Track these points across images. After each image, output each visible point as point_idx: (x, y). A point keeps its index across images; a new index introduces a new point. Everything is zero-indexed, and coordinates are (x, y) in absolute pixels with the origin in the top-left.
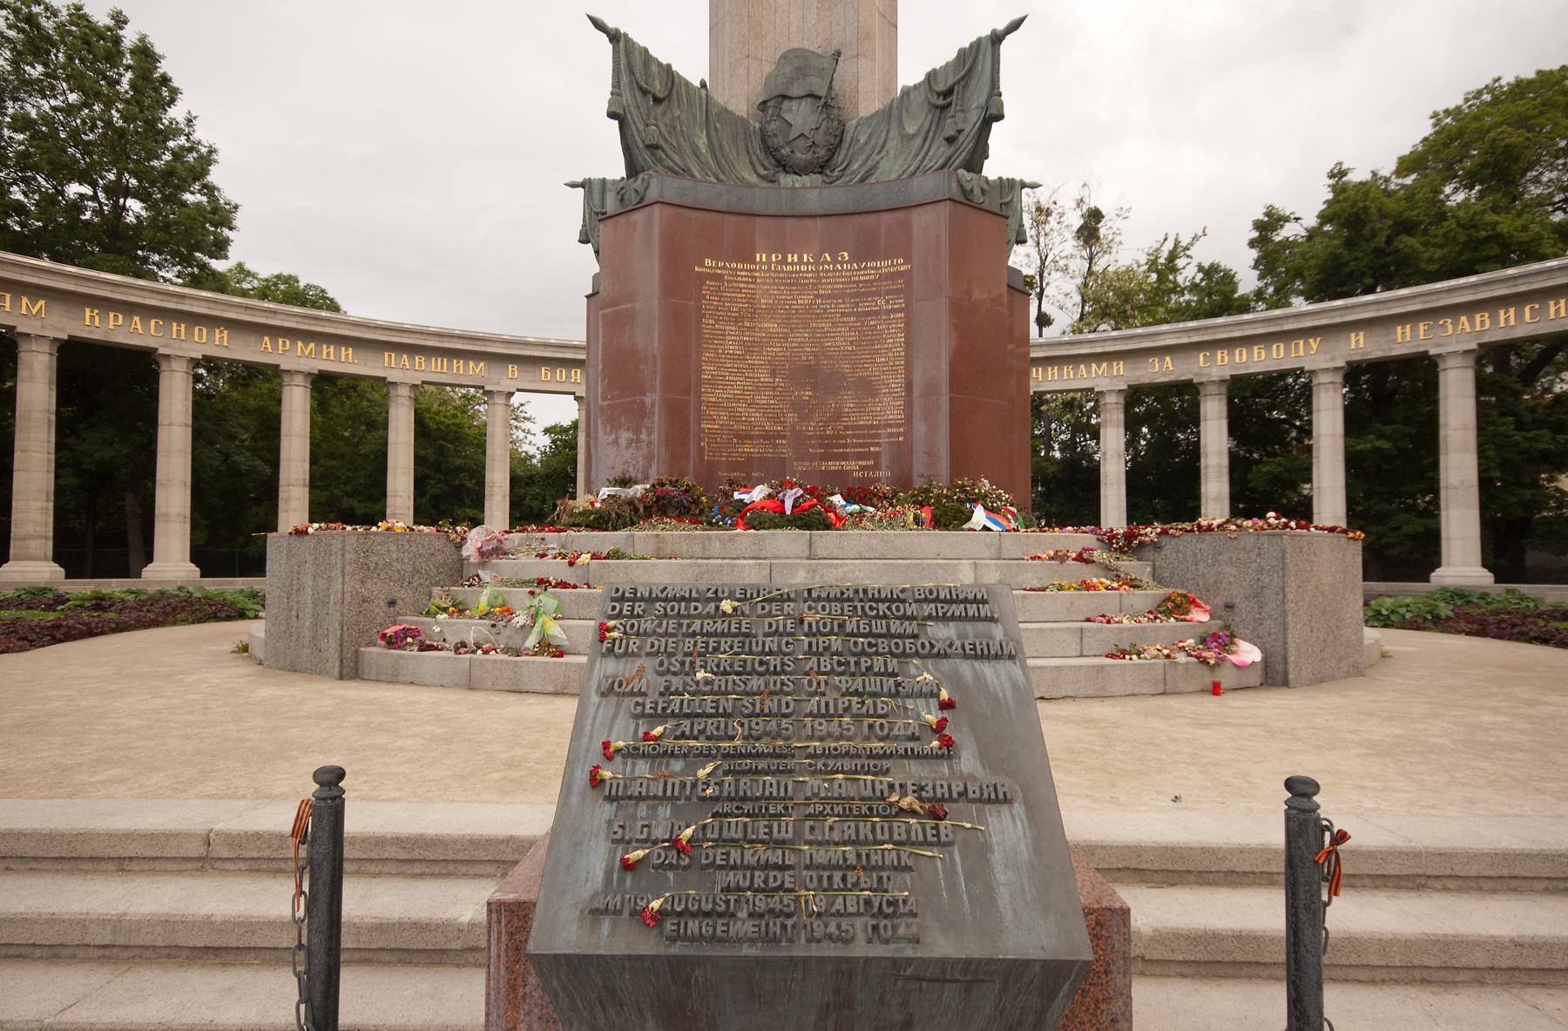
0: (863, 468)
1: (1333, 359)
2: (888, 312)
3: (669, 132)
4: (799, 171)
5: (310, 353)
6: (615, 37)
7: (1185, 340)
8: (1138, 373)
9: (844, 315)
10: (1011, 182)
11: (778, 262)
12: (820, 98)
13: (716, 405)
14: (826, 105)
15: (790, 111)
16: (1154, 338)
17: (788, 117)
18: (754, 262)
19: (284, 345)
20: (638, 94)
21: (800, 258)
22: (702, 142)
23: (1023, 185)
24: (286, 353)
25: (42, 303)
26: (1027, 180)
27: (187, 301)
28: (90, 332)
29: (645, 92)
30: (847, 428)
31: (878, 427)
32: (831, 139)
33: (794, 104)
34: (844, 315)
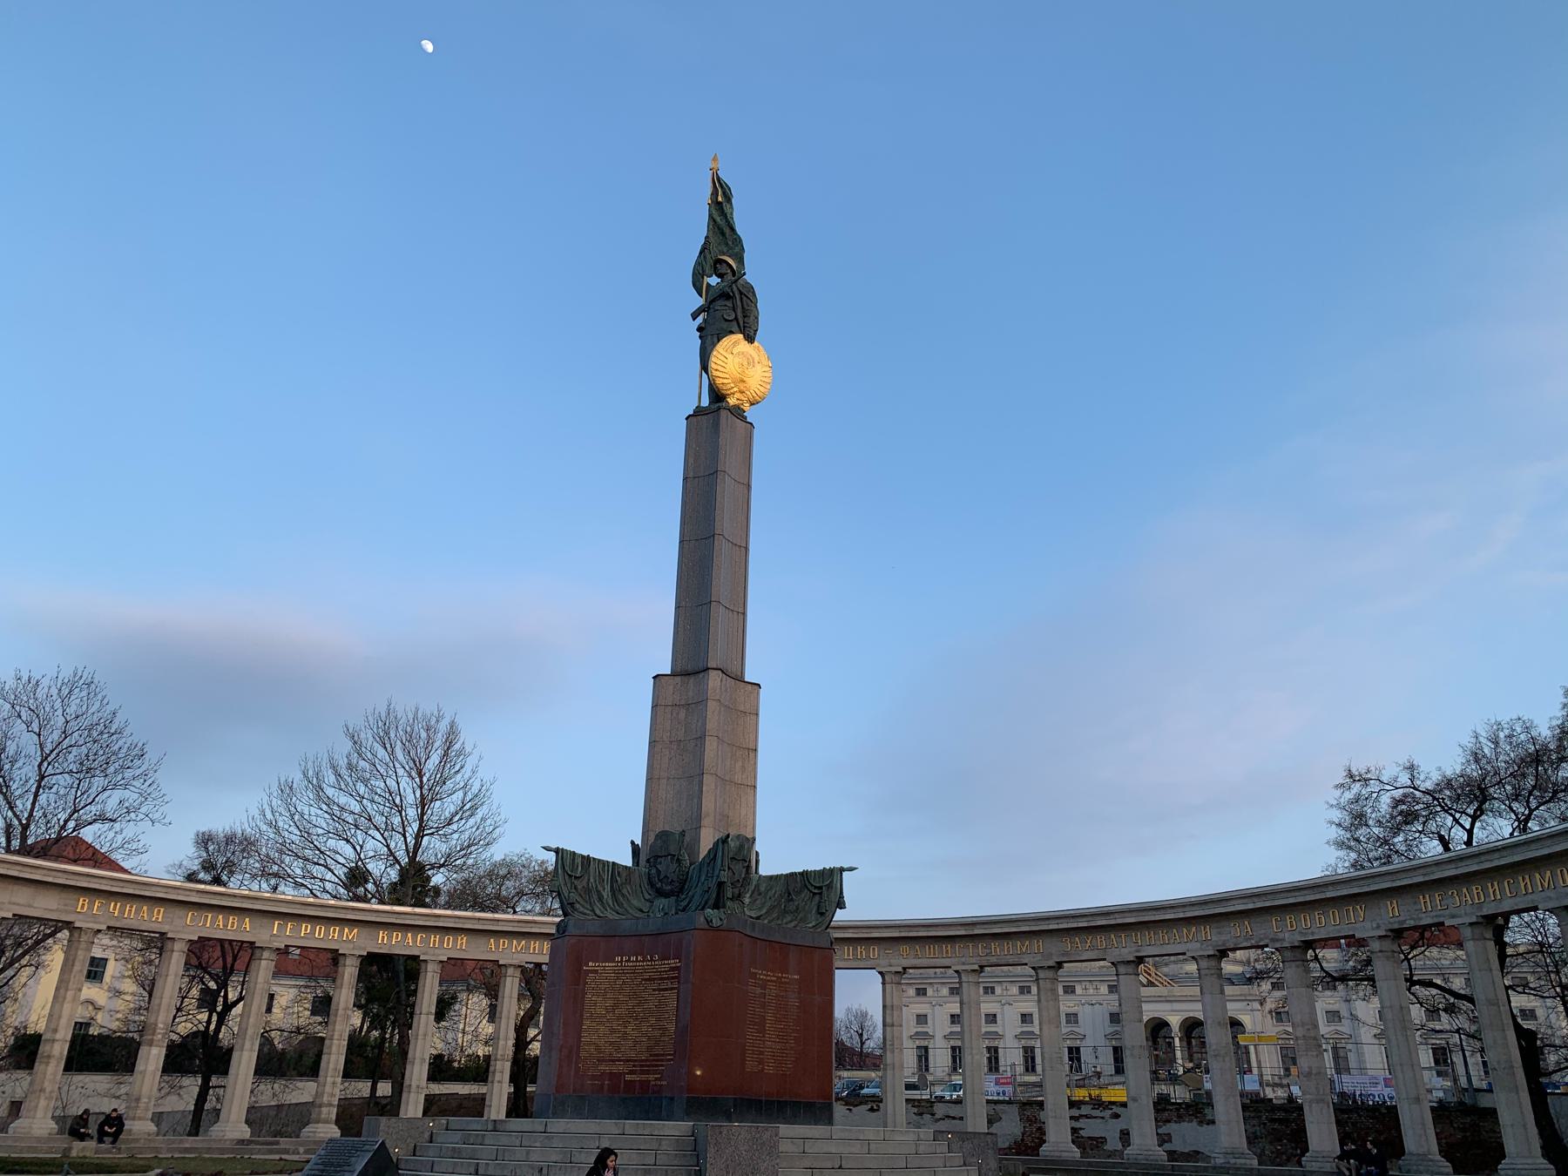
0: (656, 1079)
1: (1378, 927)
2: (672, 989)
3: (585, 893)
4: (666, 895)
5: (522, 949)
6: (557, 851)
7: (1251, 906)
8: (1223, 938)
9: (654, 990)
10: (832, 871)
11: (626, 961)
12: (674, 856)
13: (589, 1044)
14: (678, 859)
15: (660, 863)
16: (1224, 904)
17: (659, 867)
18: (614, 962)
19: (504, 945)
20: (567, 877)
21: (637, 958)
22: (606, 893)
23: (842, 870)
24: (506, 951)
25: (356, 930)
26: (845, 867)
27: (442, 919)
28: (380, 948)
29: (570, 876)
30: (651, 1055)
31: (663, 1055)
32: (681, 877)
33: (662, 860)
34: (654, 990)
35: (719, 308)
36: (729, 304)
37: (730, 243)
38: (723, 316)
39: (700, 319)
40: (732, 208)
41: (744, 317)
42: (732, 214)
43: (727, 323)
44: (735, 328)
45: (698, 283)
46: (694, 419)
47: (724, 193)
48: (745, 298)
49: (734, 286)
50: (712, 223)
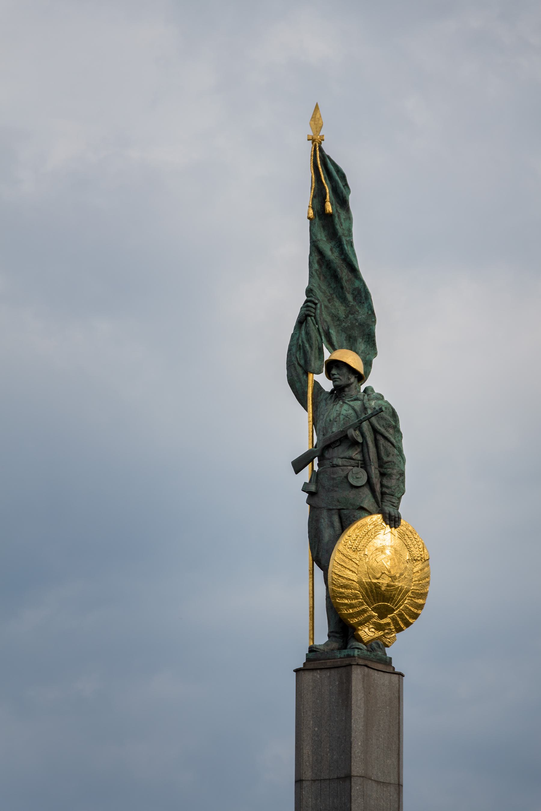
35: (340, 462)
36: (356, 454)
37: (350, 297)
38: (346, 477)
39: (306, 474)
40: (349, 218)
41: (383, 475)
42: (350, 231)
43: (354, 491)
44: (368, 502)
45: (298, 385)
46: (308, 677)
47: (335, 190)
48: (382, 441)
49: (365, 425)
50: (316, 258)
